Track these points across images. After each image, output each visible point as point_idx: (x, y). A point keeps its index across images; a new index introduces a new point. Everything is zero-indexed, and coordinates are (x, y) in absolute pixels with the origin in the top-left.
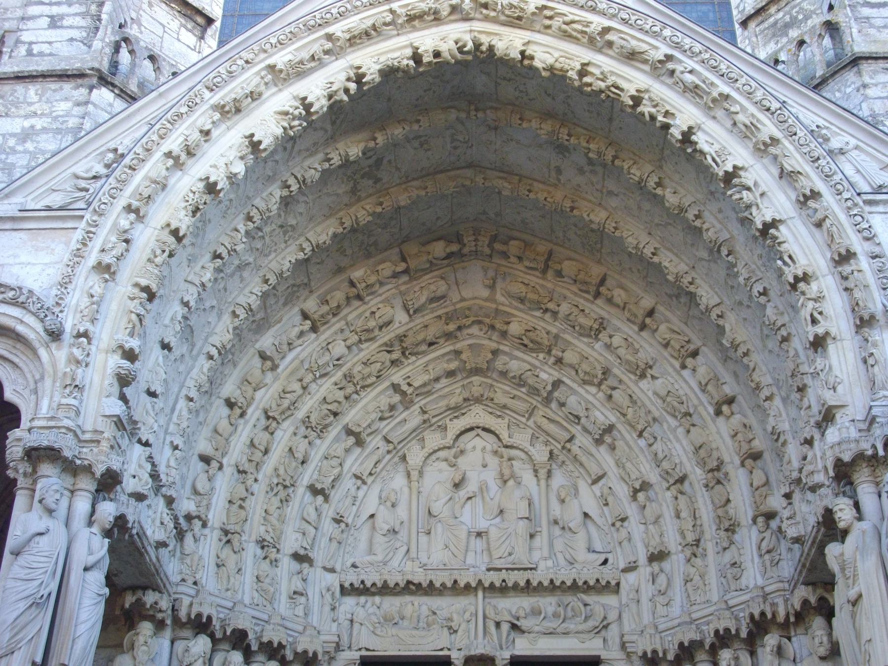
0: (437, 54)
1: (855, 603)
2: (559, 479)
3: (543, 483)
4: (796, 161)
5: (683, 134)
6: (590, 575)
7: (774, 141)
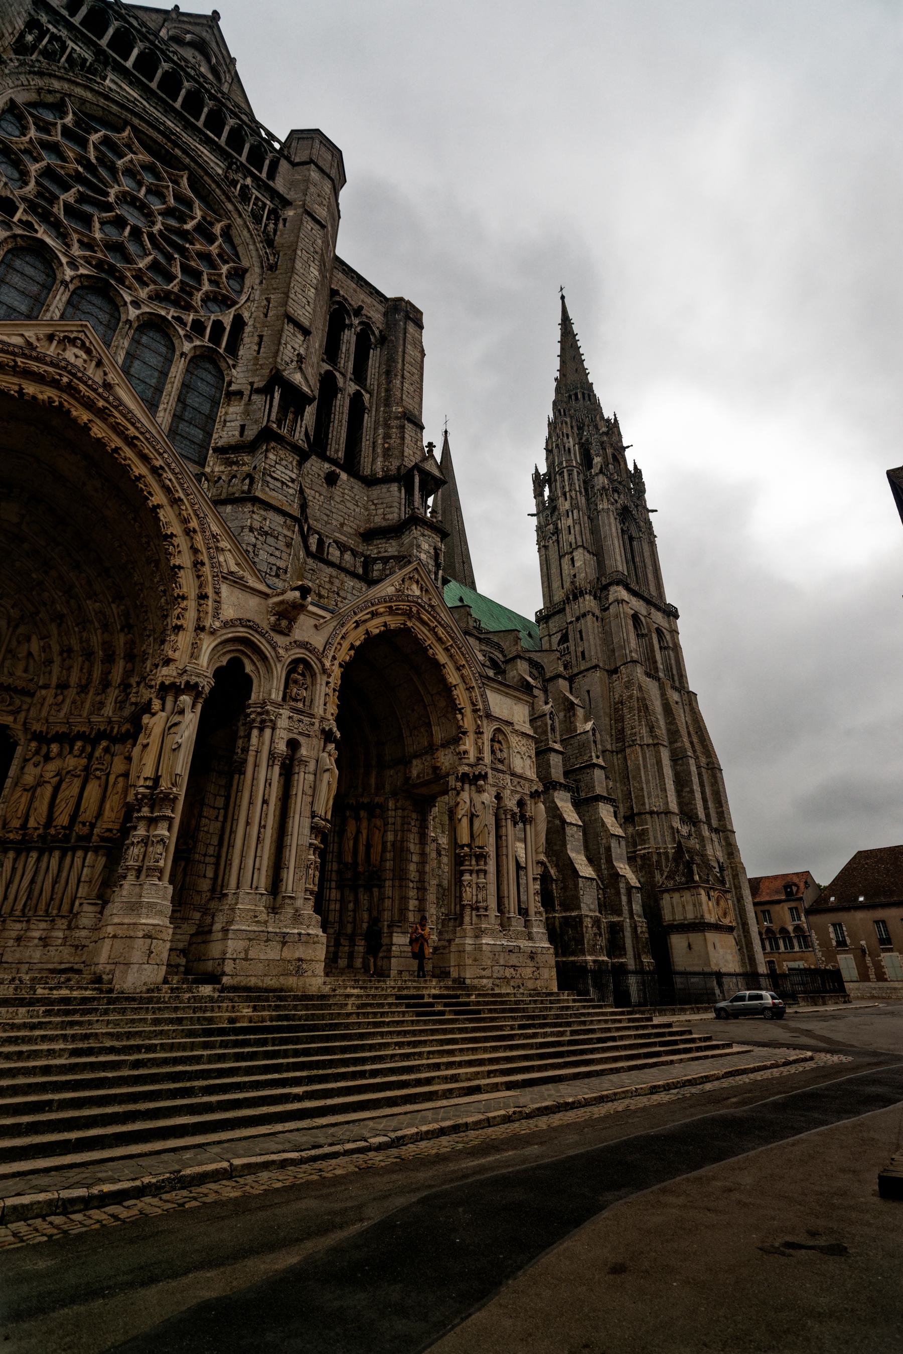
0: (34, 398)
1: (145, 746)
2: (21, 629)
3: (11, 629)
5: (153, 505)
6: (20, 684)
7: (195, 531)
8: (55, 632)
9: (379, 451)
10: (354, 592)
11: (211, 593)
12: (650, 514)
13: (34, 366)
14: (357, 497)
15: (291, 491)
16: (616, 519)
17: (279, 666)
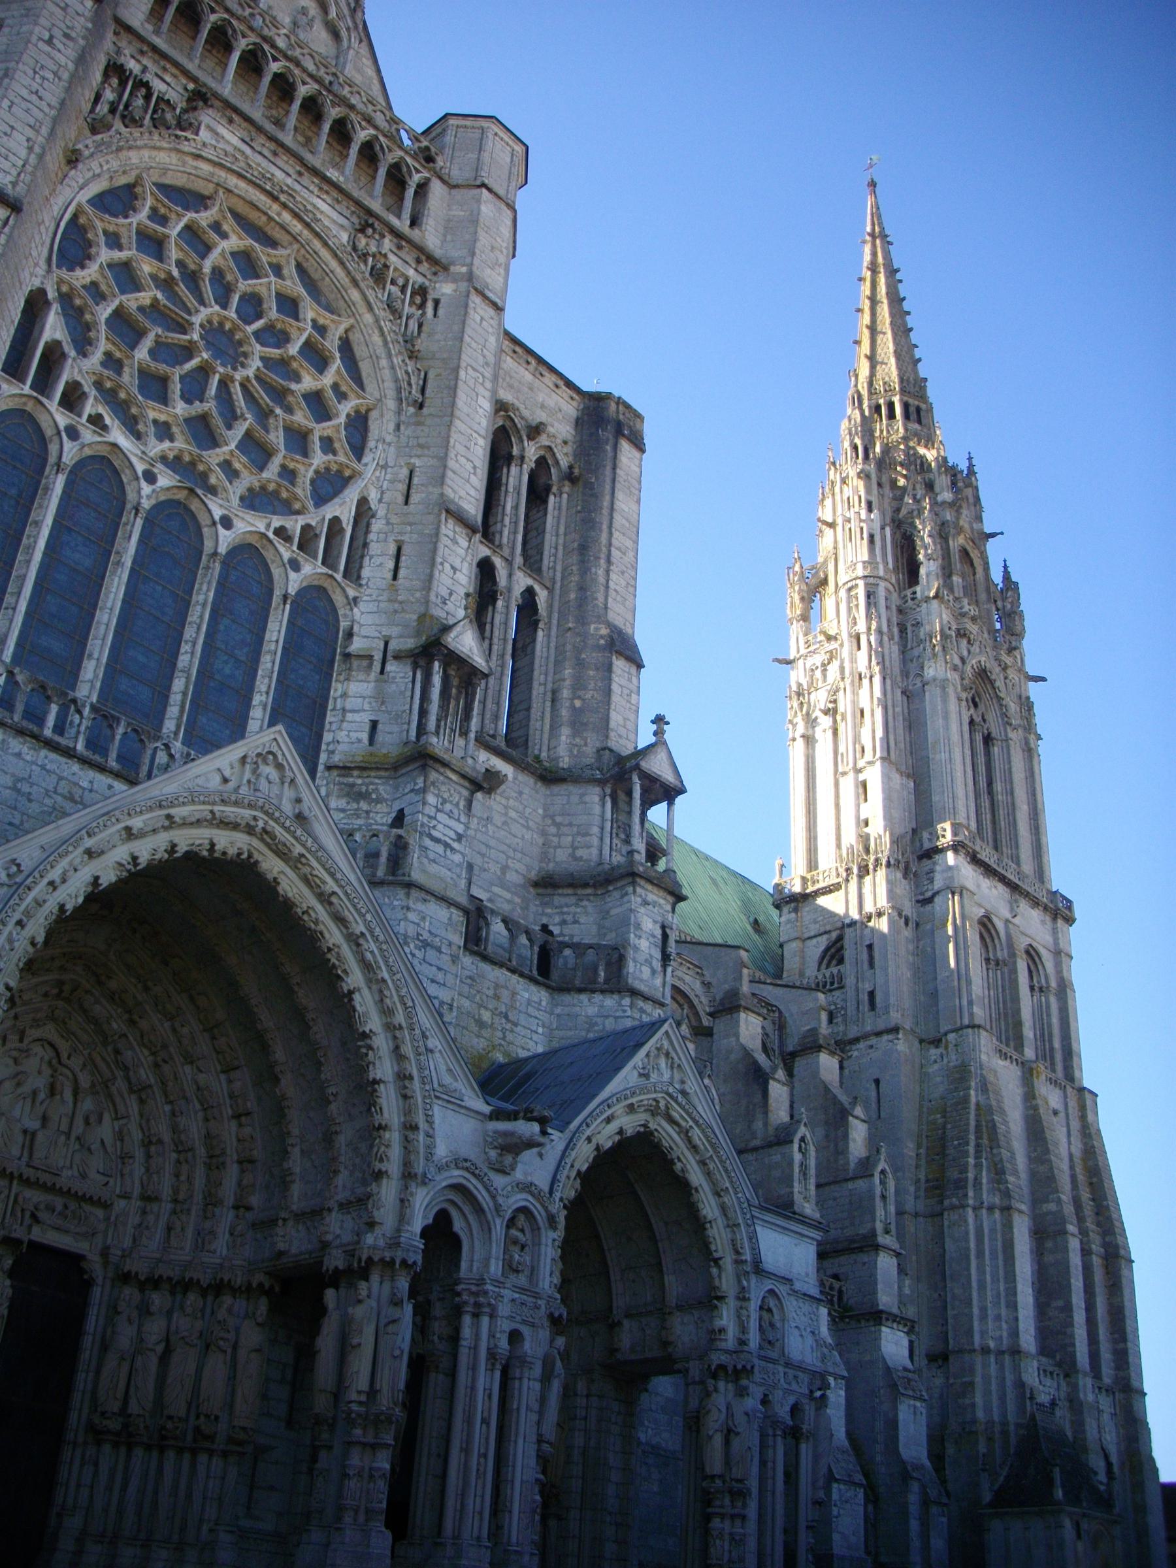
0: (224, 853)
4: (407, 1049)
8: (134, 1107)
9: (564, 713)
10: (531, 1010)
11: (423, 1125)
12: (1031, 684)
13: (230, 811)
14: (528, 810)
15: (457, 858)
16: (960, 700)
17: (498, 1221)
